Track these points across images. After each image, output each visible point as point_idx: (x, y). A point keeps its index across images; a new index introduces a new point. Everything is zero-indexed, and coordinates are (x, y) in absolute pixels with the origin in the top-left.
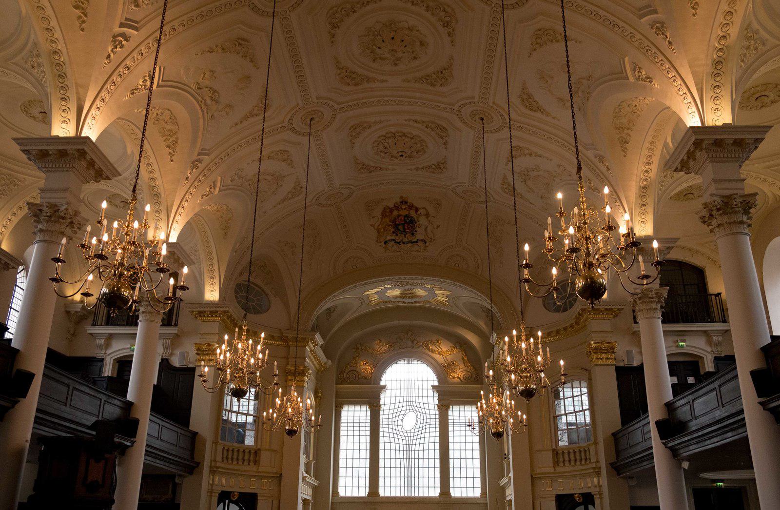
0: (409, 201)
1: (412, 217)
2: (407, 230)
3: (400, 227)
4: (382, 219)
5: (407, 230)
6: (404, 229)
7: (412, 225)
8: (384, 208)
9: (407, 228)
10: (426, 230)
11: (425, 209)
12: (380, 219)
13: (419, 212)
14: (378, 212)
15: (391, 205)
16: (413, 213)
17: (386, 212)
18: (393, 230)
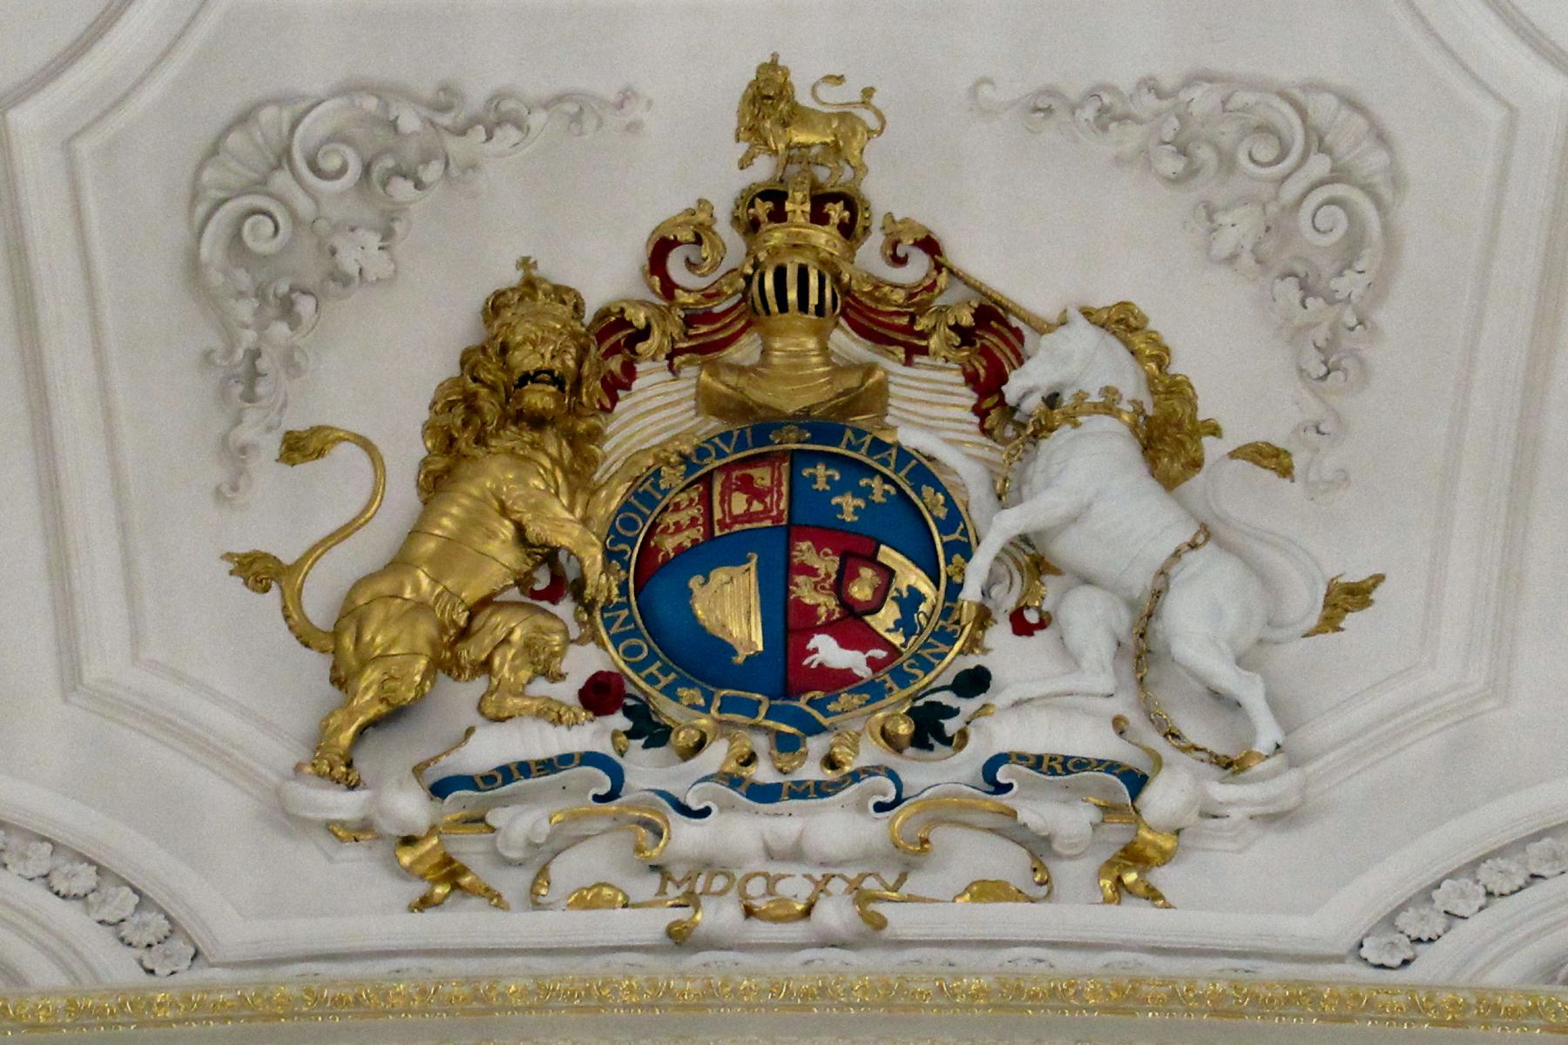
0: (888, 193)
1: (923, 472)
2: (827, 651)
3: (731, 609)
4: (435, 483)
5: (827, 651)
6: (789, 625)
7: (911, 577)
8: (495, 307)
9: (826, 604)
10: (1143, 649)
11: (1122, 323)
12: (403, 493)
13: (1025, 384)
14: (388, 365)
15: (607, 276)
16: (926, 409)
17: (522, 385)
18: (584, 662)
